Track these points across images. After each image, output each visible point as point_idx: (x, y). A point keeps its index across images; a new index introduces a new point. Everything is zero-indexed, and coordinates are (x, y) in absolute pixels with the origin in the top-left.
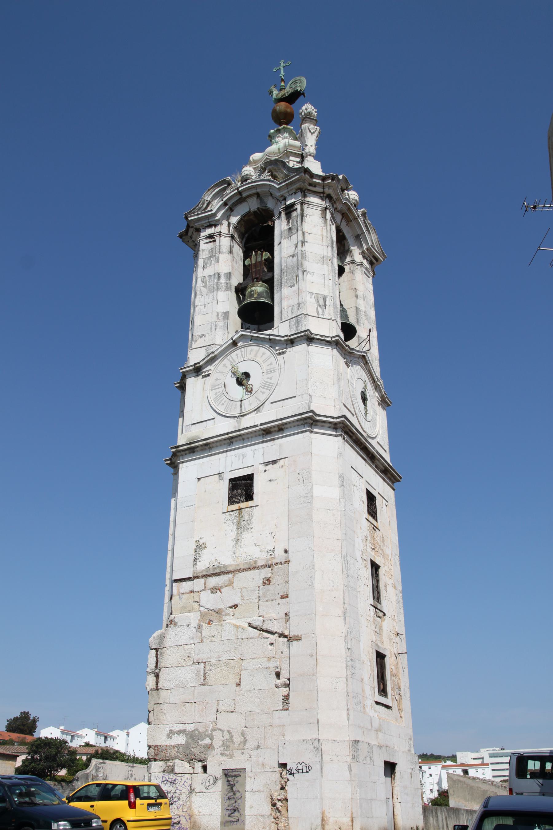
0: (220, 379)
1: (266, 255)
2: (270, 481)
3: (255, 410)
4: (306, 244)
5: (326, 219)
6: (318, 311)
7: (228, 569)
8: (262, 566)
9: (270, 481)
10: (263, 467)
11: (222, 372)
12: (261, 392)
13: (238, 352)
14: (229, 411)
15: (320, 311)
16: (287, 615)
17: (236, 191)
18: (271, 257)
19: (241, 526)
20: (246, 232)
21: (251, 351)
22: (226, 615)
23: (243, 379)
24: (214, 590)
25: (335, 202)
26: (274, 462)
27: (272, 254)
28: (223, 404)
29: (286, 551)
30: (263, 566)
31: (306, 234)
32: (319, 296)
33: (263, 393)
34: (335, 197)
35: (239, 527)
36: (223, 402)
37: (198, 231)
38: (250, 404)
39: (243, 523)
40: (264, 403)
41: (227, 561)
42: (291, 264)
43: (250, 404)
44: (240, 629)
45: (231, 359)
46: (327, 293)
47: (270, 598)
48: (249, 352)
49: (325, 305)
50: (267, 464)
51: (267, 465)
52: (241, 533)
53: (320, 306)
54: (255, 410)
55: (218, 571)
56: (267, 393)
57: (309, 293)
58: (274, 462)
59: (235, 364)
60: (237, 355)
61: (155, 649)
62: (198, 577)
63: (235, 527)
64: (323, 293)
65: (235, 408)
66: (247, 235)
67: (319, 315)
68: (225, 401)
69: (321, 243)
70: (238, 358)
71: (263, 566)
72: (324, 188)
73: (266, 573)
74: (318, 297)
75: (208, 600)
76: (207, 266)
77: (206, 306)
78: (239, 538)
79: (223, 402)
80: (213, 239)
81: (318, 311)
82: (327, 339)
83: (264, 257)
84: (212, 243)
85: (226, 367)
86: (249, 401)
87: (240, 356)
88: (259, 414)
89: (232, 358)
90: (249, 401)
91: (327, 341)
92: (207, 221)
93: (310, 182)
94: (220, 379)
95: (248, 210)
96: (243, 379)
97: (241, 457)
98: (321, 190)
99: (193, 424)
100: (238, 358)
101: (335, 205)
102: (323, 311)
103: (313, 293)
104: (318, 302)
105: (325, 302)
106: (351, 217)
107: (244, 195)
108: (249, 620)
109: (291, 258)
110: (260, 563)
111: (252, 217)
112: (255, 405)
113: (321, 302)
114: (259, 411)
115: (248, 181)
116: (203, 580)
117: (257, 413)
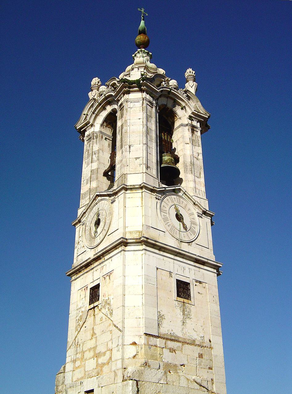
2: (199, 293)
7: (180, 340)
8: (198, 345)
9: (199, 293)
10: (195, 283)
14: (172, 233)
16: (212, 380)
17: (169, 90)
19: (186, 315)
22: (179, 370)
24: (172, 350)
26: (200, 282)
29: (210, 341)
30: (199, 345)
33: (191, 235)
35: (184, 314)
36: (169, 224)
39: (186, 312)
41: (179, 334)
44: (189, 382)
47: (203, 367)
50: (197, 281)
51: (196, 282)
52: (185, 319)
55: (173, 338)
58: (200, 282)
61: (135, 380)
62: (161, 338)
63: (182, 313)
71: (199, 345)
73: (198, 350)
75: (168, 357)
78: (185, 322)
79: (169, 224)
97: (183, 269)
107: (170, 95)
108: (194, 377)
110: (197, 343)
115: (175, 90)
116: (164, 341)
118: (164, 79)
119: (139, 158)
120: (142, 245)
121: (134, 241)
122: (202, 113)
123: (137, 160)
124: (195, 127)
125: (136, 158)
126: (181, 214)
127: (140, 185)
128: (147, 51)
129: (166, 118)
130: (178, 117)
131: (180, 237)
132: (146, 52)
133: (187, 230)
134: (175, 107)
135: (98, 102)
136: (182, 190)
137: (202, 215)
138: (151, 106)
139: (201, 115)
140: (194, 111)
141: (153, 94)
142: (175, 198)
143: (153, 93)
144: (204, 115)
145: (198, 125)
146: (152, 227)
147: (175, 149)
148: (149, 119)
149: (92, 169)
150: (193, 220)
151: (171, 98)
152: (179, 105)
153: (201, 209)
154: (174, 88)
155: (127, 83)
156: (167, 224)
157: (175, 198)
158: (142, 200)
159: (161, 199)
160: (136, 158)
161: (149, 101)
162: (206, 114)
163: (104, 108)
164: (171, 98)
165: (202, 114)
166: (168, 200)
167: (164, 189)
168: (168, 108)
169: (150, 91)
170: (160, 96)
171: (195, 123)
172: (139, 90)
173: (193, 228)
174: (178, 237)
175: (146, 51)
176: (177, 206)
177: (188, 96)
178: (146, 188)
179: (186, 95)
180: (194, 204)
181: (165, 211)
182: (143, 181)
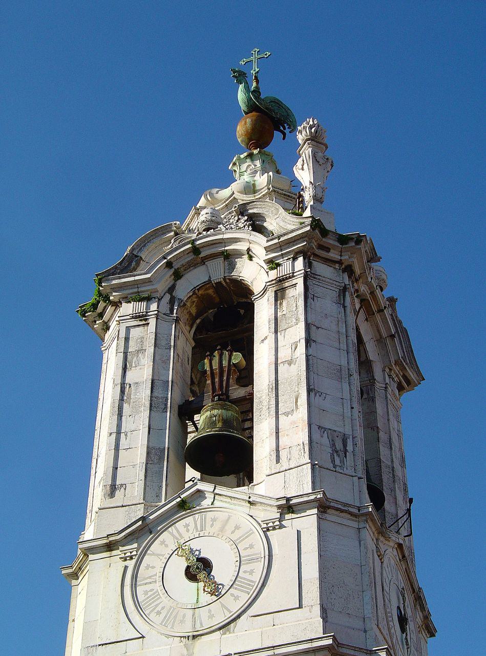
0: (153, 567)
1: (237, 358)
3: (220, 629)
4: (313, 344)
5: (344, 307)
6: (333, 461)
11: (158, 555)
12: (232, 595)
13: (189, 520)
15: (337, 462)
17: (190, 246)
18: (244, 363)
20: (198, 315)
21: (214, 520)
23: (198, 570)
25: (357, 280)
27: (249, 354)
28: (159, 613)
31: (313, 328)
32: (336, 434)
33: (236, 598)
34: (358, 271)
36: (159, 608)
37: (117, 305)
38: (211, 616)
40: (239, 617)
42: (286, 376)
43: (211, 616)
45: (175, 532)
46: (348, 430)
48: (209, 523)
49: (346, 451)
53: (337, 452)
54: (220, 629)
56: (244, 598)
57: (319, 427)
59: (182, 541)
60: (187, 526)
64: (341, 430)
65: (182, 622)
66: (198, 321)
67: (335, 466)
68: (163, 608)
69: (336, 345)
70: (188, 531)
72: (341, 256)
74: (333, 437)
76: (131, 366)
77: (129, 434)
79: (159, 608)
80: (144, 322)
81: (333, 461)
82: (351, 510)
83: (234, 361)
84: (141, 328)
85: (167, 546)
86: (210, 611)
87: (192, 526)
88: (228, 635)
89: (178, 531)
90: (210, 611)
91: (351, 514)
92: (136, 290)
93: (321, 243)
94: (153, 567)
95: (207, 279)
96: (198, 570)
98: (338, 257)
99: (99, 645)
100: (188, 531)
101: (355, 284)
102: (342, 462)
103: (325, 429)
104: (334, 445)
105: (345, 445)
106: (374, 308)
109: (286, 365)
111: (211, 292)
112: (221, 618)
113: (339, 446)
114: (229, 630)
117: (224, 634)
118: (172, 231)
122: (293, 227)
124: (283, 280)
128: (245, 154)
132: (246, 157)
134: (232, 267)
136: (207, 491)
138: (144, 322)
140: (268, 241)
141: (143, 292)
146: (103, 645)
152: (239, 254)
154: (204, 231)
155: (87, 313)
156: (154, 609)
161: (133, 318)
162: (301, 223)
165: (292, 231)
167: (140, 523)
169: (131, 291)
172: (114, 307)
175: (242, 156)
179: (246, 218)
181: (150, 577)
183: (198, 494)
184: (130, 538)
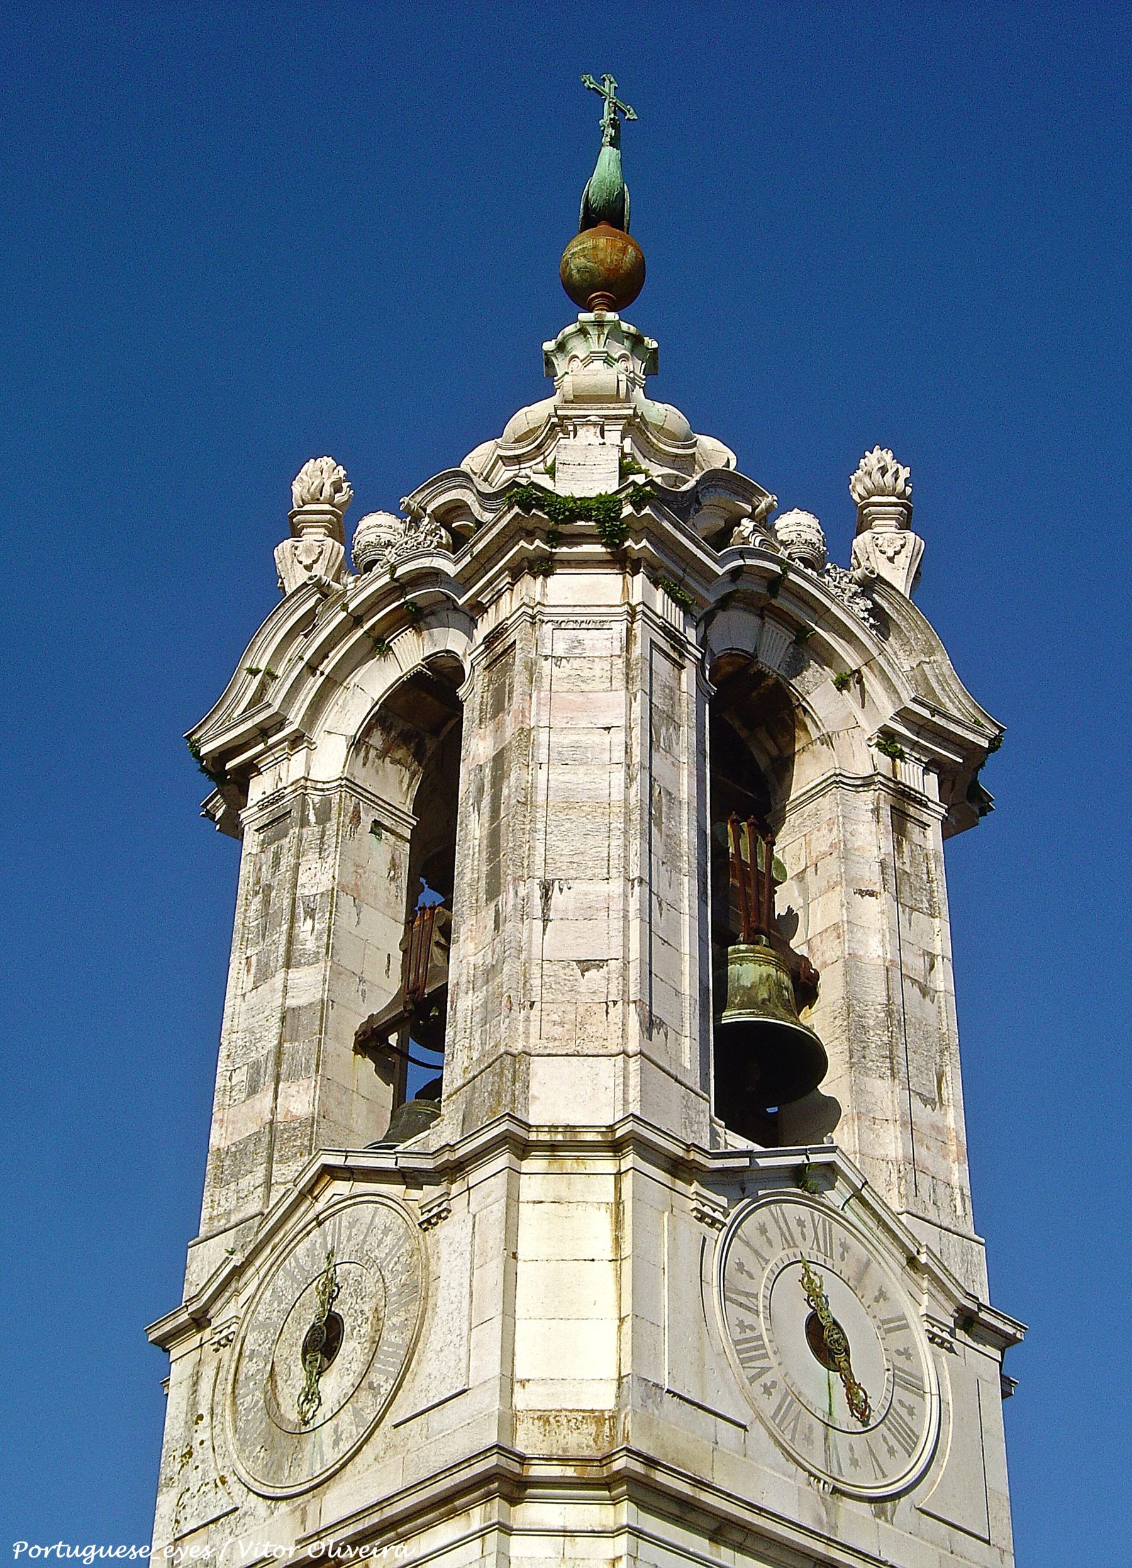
3: (871, 1500)
33: (891, 1451)
36: (767, 1379)
54: (871, 1500)
79: (767, 1379)
107: (781, 602)
115: (809, 571)
118: (750, 502)
119: (599, 964)
120: (615, 1501)
121: (570, 1472)
122: (958, 715)
123: (592, 973)
124: (915, 800)
125: (586, 966)
126: (835, 1323)
127: (611, 1128)
128: (633, 329)
129: (743, 734)
130: (814, 734)
131: (828, 1461)
132: (629, 336)
133: (872, 1422)
134: (797, 667)
135: (345, 607)
136: (845, 1177)
137: (952, 1333)
139: (953, 727)
140: (914, 700)
141: (687, 586)
142: (801, 1223)
143: (687, 579)
144: (967, 728)
145: (929, 786)
146: (675, 1394)
147: (791, 918)
148: (663, 730)
149: (291, 1002)
150: (900, 1361)
151: (783, 618)
152: (827, 657)
153: (949, 1296)
154: (802, 559)
155: (542, 510)
156: (759, 1375)
157: (801, 1223)
158: (618, 1224)
159: (728, 1221)
160: (586, 966)
162: (977, 722)
163: (378, 645)
164: (783, 618)
165: (958, 722)
166: (763, 1230)
167: (746, 1162)
168: (762, 675)
169: (672, 566)
170: (724, 603)
171: (912, 774)
172: (609, 557)
173: (903, 1412)
174: (817, 1461)
175: (624, 326)
176: (812, 1267)
177: (876, 612)
178: (646, 1150)
179: (870, 605)
180: (912, 1261)
182: (626, 1102)
183: (823, 1171)
184: (717, 1177)
